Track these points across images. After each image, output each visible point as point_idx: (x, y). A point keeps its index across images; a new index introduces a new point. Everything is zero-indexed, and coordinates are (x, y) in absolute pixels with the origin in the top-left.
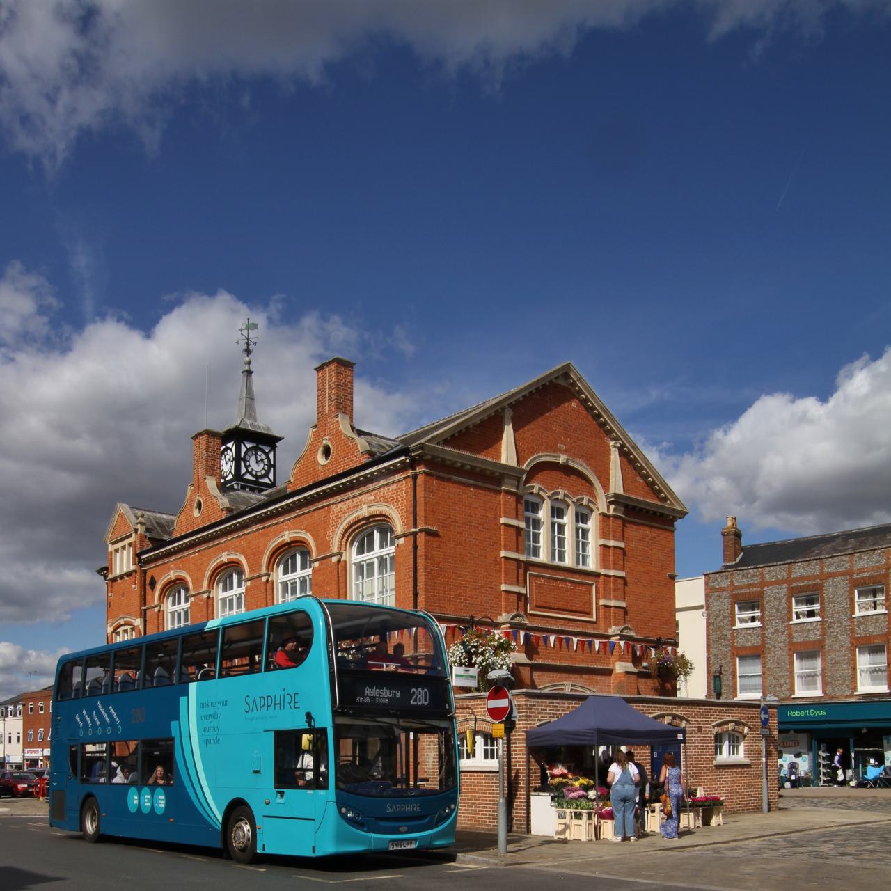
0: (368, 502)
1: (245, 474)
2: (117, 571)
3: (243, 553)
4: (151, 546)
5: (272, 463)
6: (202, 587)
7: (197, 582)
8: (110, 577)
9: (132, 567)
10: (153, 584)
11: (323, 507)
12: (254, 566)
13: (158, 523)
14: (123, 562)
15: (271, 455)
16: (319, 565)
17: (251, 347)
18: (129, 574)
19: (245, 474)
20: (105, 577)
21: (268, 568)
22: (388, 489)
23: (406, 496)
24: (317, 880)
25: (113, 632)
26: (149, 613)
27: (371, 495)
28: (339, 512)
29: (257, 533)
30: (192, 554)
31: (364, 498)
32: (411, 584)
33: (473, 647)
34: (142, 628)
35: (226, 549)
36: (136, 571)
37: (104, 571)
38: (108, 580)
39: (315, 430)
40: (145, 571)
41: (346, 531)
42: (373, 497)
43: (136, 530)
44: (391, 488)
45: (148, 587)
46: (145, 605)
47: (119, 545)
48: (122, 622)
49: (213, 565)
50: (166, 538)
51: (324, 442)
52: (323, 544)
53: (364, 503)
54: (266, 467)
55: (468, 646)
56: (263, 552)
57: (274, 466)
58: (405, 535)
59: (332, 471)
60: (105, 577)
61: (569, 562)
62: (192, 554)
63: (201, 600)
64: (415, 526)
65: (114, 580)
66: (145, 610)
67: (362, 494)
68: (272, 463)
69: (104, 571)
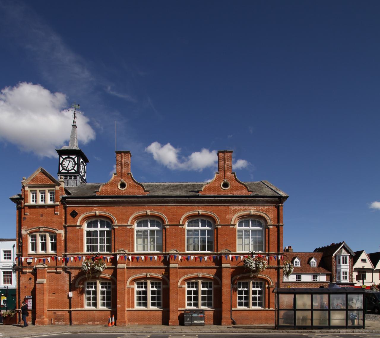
2: (31, 202)
3: (164, 213)
5: (61, 165)
8: (26, 204)
9: (49, 202)
10: (74, 215)
23: (274, 212)
25: (28, 234)
26: (69, 229)
30: (116, 207)
32: (276, 242)
34: (63, 234)
36: (57, 205)
37: (19, 201)
42: (255, 208)
44: (266, 207)
48: (42, 229)
56: (182, 216)
58: (273, 225)
62: (116, 206)
65: (31, 207)
68: (61, 165)
69: (19, 201)
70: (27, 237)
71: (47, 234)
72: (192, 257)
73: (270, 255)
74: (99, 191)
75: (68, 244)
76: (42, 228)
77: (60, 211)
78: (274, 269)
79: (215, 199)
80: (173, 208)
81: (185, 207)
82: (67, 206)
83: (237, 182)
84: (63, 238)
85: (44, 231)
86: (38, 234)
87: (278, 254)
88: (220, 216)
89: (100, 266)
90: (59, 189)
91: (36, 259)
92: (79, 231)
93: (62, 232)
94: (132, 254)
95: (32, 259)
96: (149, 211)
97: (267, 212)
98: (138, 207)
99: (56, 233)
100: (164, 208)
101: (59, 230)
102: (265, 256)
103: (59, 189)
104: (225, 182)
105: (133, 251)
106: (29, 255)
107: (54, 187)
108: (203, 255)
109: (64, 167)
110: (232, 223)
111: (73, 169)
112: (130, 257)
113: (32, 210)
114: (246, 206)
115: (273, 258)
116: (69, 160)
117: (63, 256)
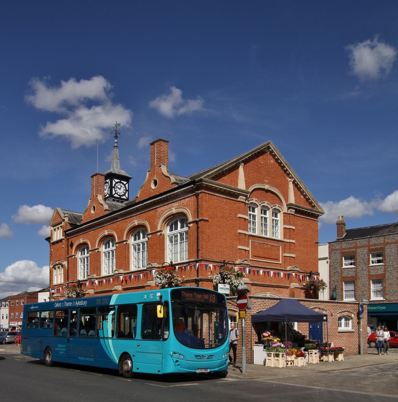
0: (175, 207)
1: (114, 194)
2: (55, 239)
3: (115, 231)
4: (70, 228)
5: (127, 189)
6: (95, 246)
7: (93, 244)
8: (52, 242)
9: (62, 237)
10: (72, 245)
11: (153, 209)
12: (120, 236)
13: (74, 217)
14: (58, 235)
15: (127, 186)
16: (152, 236)
17: (118, 135)
18: (61, 241)
19: (114, 194)
20: (49, 242)
21: (126, 237)
22: (185, 200)
23: (194, 204)
24: (157, 386)
25: (53, 268)
26: (70, 258)
27: (177, 203)
28: (161, 211)
29: (122, 221)
31: (173, 204)
32: (196, 245)
33: (226, 275)
34: (66, 265)
35: (107, 229)
36: (63, 239)
38: (51, 243)
39: (150, 173)
40: (68, 239)
41: (164, 220)
42: (178, 204)
43: (64, 220)
44: (186, 200)
45: (69, 247)
46: (68, 255)
47: (56, 227)
48: (57, 263)
49: (130, 226)
50: (78, 224)
51: (154, 178)
52: (154, 226)
53: (173, 207)
54: (124, 191)
55: (223, 274)
57: (128, 191)
58: (193, 222)
59: (158, 192)
60: (49, 242)
61: (268, 236)
63: (95, 253)
64: (198, 218)
66: (68, 258)
67: (172, 203)
68: (127, 189)
70: (52, 270)
71: (60, 266)
72: (133, 276)
73: (190, 264)
74: (82, 220)
75: (69, 274)
76: (57, 261)
77: (63, 245)
78: (195, 283)
79: (144, 204)
80: (119, 223)
81: (127, 219)
82: (68, 239)
83: (163, 176)
84: (67, 268)
85: (59, 264)
86: (56, 266)
87: (196, 261)
88: (150, 223)
89: (72, 293)
90: (64, 225)
91: (56, 289)
92: (74, 260)
93: (65, 263)
94: (99, 278)
95: (54, 289)
96: (107, 231)
97: (184, 206)
98: (101, 229)
99: (63, 265)
100: (115, 225)
101: (64, 262)
102: (187, 266)
103: (64, 225)
104: (154, 179)
105: (100, 275)
106: (53, 286)
107: (61, 223)
108: (140, 272)
109: (117, 193)
110: (159, 229)
111: (116, 193)
112: (96, 282)
113: (54, 246)
114: (170, 204)
115: (193, 267)
116: (120, 185)
117: (67, 285)
